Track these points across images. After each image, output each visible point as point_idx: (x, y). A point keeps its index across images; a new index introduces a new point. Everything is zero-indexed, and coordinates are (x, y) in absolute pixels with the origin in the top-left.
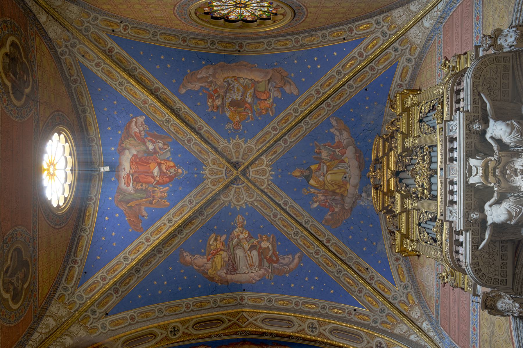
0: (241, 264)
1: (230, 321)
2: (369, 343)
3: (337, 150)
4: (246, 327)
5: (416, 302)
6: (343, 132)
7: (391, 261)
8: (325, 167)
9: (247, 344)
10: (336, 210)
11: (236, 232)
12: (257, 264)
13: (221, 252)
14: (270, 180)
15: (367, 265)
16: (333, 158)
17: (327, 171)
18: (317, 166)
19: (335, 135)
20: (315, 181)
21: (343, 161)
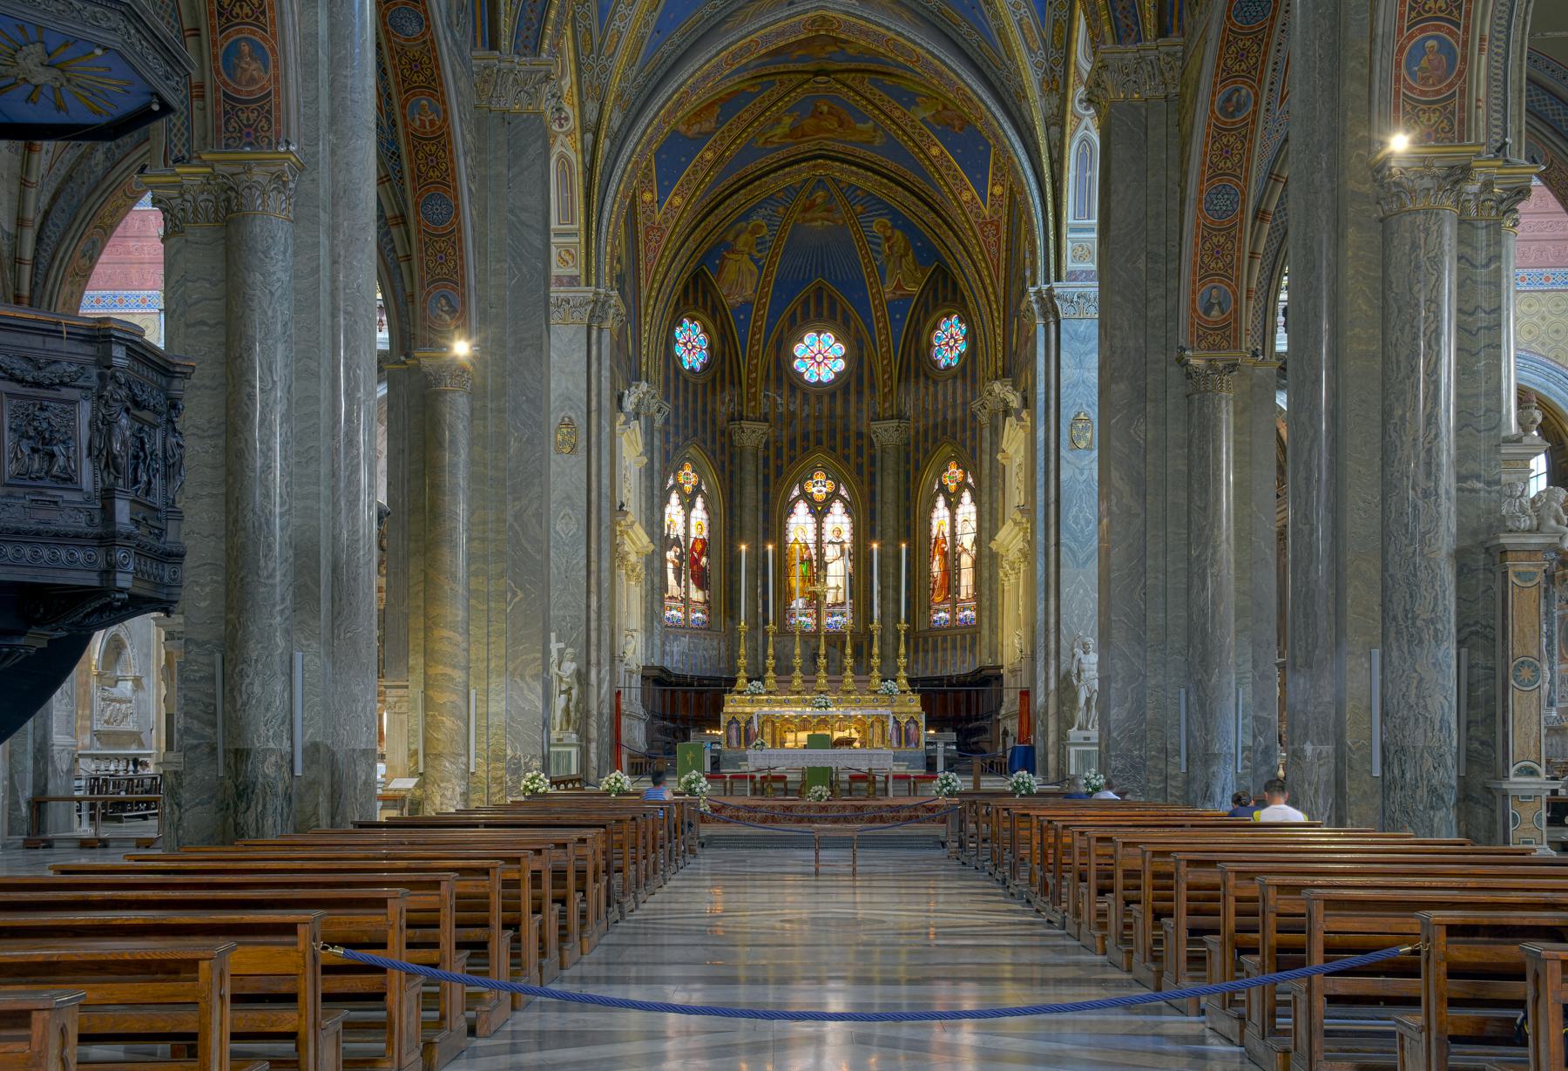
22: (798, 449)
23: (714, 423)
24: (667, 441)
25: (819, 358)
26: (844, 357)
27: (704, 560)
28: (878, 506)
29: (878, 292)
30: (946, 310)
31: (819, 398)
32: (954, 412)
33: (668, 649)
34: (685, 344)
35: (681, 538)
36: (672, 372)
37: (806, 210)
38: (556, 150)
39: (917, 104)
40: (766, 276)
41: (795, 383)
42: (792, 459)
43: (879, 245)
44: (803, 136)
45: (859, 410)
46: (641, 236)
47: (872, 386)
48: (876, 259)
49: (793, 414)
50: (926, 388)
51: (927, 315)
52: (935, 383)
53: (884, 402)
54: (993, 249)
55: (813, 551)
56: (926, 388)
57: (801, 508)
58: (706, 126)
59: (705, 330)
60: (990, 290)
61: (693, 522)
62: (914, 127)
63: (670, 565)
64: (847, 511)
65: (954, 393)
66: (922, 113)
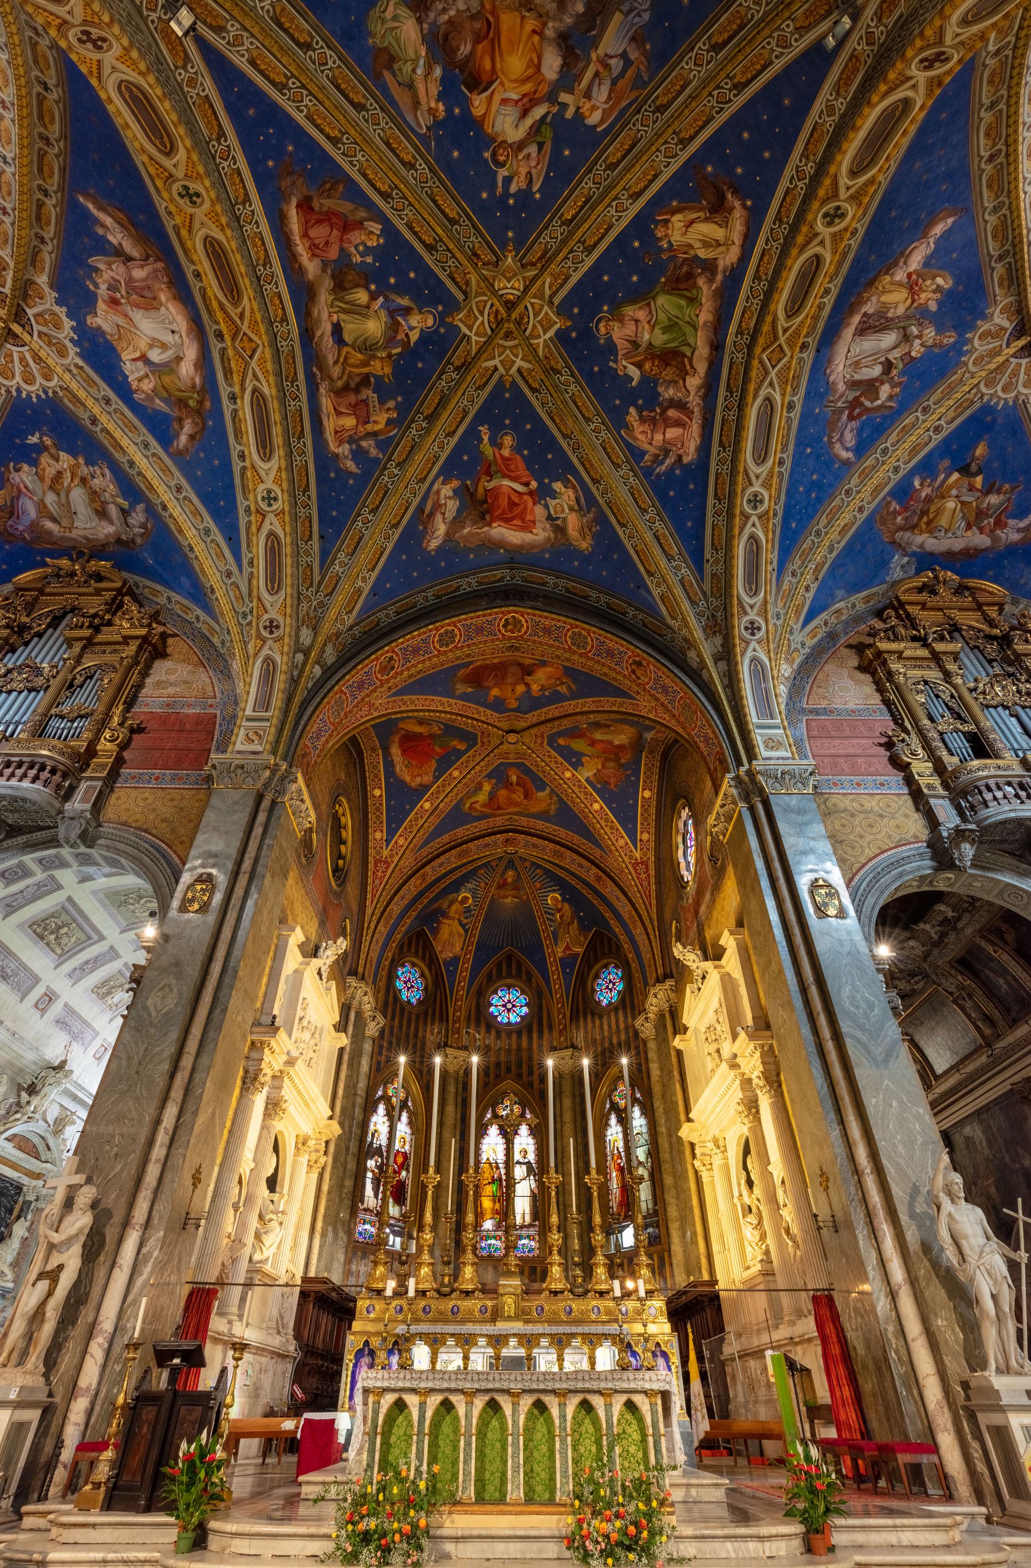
0: (870, 344)
1: (785, 331)
2: (752, 607)
3: (992, 520)
4: (761, 362)
5: (795, 666)
6: (1022, 535)
7: (824, 616)
8: (971, 499)
9: (711, 354)
10: (899, 519)
11: (930, 333)
12: (857, 377)
13: (909, 301)
14: (990, 400)
15: (820, 577)
16: (981, 514)
17: (962, 502)
18: (979, 486)
19: (1021, 520)
20: (956, 481)
21: (969, 527)
24: (380, 1053)
25: (509, 1006)
26: (526, 1005)
30: (604, 962)
31: (509, 1034)
32: (619, 1036)
33: (354, 1267)
36: (391, 1000)
37: (500, 887)
38: (265, 651)
39: (582, 765)
41: (490, 1024)
44: (499, 808)
46: (371, 866)
47: (550, 1027)
50: (593, 1022)
51: (590, 969)
52: (601, 1017)
54: (645, 883)
55: (503, 1171)
56: (593, 1022)
57: (493, 1131)
58: (427, 779)
59: (422, 975)
62: (580, 787)
63: (369, 1175)
65: (617, 1022)
66: (587, 772)
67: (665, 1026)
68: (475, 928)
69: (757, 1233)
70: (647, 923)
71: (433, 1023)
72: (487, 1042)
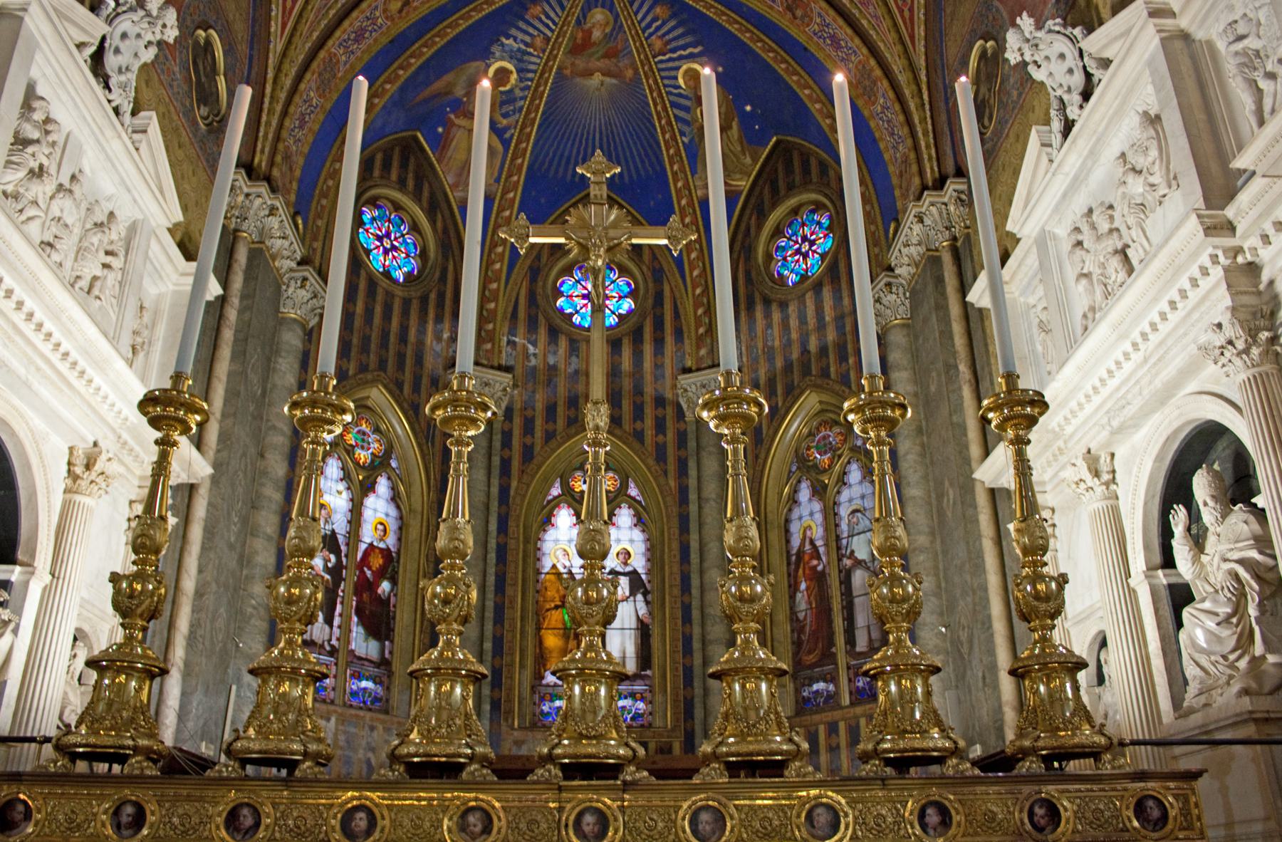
22: (561, 422)
23: (419, 360)
26: (633, 294)
27: (385, 586)
28: (693, 508)
29: (686, 185)
30: (793, 202)
34: (379, 238)
35: (341, 539)
37: (578, 49)
40: (513, 159)
42: (549, 436)
43: (687, 109)
45: (658, 366)
47: (679, 334)
48: (682, 134)
49: (553, 369)
50: (768, 316)
52: (783, 305)
53: (698, 348)
56: (768, 316)
59: (415, 228)
60: (897, 65)
61: (368, 514)
64: (640, 522)
67: (940, 281)
68: (524, 137)
69: (1229, 636)
70: (903, 78)
71: (439, 319)
72: (551, 360)
